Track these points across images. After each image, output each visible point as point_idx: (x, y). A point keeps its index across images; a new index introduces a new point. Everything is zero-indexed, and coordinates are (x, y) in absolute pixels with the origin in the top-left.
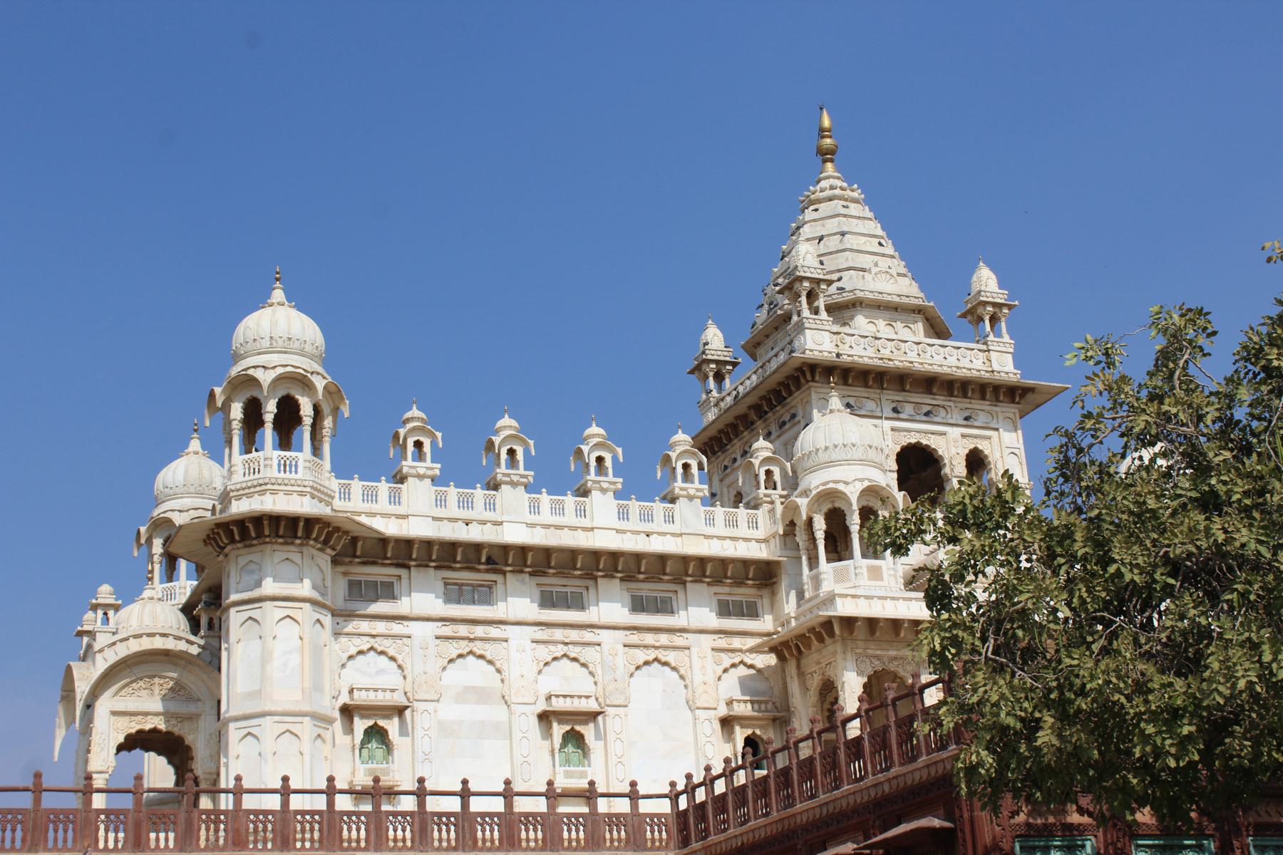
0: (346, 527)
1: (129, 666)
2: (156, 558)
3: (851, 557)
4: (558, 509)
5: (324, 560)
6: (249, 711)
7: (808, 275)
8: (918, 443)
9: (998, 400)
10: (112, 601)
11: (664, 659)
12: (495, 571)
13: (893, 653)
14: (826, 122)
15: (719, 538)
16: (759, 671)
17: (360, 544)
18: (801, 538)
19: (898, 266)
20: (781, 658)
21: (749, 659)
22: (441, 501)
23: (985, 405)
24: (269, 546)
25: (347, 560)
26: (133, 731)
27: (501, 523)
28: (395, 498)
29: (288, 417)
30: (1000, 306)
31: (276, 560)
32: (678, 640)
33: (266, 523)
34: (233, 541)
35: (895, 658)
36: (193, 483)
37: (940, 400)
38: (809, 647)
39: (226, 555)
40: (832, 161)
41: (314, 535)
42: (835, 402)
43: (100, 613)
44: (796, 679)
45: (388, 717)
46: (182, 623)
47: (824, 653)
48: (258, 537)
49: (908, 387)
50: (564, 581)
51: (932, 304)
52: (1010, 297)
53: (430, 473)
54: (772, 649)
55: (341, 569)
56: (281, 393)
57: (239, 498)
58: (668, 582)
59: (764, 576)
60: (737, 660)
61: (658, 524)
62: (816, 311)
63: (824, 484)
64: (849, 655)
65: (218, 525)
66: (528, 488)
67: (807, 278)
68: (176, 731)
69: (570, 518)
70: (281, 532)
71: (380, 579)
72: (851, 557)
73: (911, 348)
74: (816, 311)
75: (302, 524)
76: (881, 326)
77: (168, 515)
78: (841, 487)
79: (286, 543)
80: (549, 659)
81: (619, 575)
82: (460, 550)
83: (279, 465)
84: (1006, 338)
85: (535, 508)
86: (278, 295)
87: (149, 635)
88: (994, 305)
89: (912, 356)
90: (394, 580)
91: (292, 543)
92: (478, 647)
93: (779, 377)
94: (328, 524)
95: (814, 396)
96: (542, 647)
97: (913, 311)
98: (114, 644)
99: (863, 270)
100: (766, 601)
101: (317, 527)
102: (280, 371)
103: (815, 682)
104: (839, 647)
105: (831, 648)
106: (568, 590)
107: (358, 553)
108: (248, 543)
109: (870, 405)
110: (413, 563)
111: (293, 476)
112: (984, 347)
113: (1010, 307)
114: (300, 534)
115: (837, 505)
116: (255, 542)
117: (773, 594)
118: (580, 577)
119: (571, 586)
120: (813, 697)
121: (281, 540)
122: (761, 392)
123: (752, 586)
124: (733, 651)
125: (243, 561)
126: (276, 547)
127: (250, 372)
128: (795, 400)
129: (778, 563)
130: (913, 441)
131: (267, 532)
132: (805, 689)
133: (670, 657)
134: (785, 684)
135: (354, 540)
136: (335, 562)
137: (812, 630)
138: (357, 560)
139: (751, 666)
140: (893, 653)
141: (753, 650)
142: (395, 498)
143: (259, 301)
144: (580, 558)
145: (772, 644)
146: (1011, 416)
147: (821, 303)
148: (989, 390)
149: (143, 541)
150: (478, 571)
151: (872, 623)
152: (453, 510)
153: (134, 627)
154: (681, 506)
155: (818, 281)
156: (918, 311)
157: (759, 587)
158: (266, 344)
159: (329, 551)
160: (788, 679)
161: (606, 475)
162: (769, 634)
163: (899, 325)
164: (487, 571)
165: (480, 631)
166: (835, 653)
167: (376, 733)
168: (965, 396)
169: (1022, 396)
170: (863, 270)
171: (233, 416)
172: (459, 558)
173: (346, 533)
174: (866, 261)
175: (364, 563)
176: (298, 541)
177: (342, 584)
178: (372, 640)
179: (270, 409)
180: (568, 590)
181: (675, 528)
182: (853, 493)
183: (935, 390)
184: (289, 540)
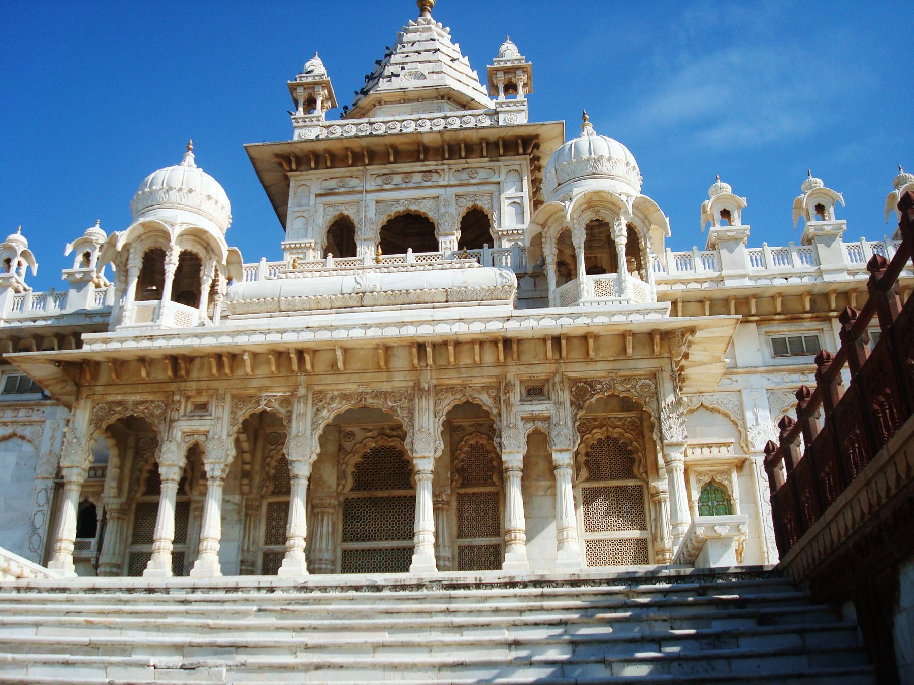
32: (36, 416)
35: (143, 402)
37: (431, 165)
88: (507, 71)
109: (354, 182)
130: (401, 208)
133: (27, 432)
140: (138, 398)
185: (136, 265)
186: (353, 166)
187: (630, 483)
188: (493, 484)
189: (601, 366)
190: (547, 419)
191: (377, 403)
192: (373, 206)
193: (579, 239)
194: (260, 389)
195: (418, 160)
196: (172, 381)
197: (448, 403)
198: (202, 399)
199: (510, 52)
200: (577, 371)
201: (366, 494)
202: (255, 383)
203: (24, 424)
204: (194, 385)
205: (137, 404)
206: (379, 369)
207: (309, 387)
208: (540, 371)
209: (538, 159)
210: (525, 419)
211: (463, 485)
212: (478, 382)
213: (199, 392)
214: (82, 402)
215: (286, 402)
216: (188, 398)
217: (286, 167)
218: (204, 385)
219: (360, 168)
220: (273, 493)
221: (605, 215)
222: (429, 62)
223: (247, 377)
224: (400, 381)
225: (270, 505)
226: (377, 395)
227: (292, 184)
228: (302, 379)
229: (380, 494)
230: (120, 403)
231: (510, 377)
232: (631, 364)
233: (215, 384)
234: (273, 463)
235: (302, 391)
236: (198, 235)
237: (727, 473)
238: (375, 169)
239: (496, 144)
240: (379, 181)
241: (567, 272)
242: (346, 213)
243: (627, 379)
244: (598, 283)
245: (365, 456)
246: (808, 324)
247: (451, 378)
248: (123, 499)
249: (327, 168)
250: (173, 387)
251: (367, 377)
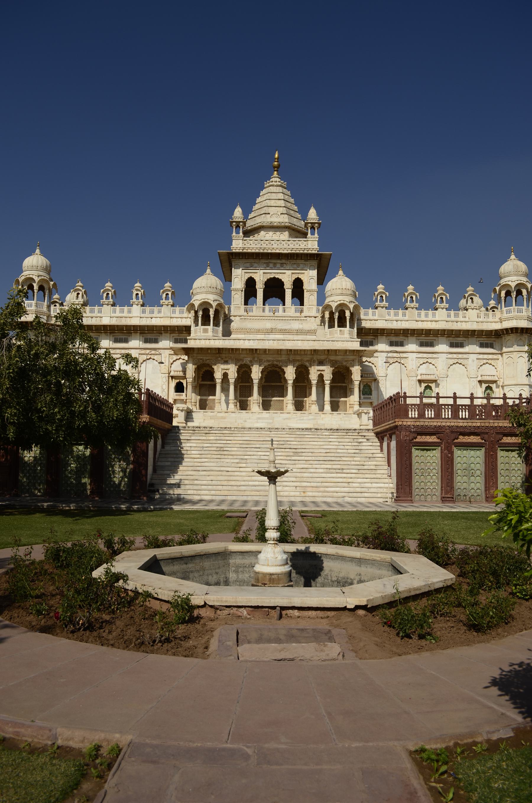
4: (122, 311)
8: (274, 278)
14: (276, 156)
23: (303, 262)
27: (102, 317)
37: (283, 261)
40: (277, 171)
61: (156, 314)
74: (237, 233)
84: (316, 235)
85: (114, 312)
86: (38, 251)
89: (275, 246)
109: (256, 265)
130: (272, 277)
139: (183, 359)
146: (314, 264)
154: (164, 309)
163: (278, 233)
181: (162, 315)
185: (200, 313)
186: (256, 259)
187: (344, 385)
188: (305, 383)
189: (339, 357)
190: (324, 371)
191: (277, 363)
192: (262, 274)
193: (336, 316)
194: (244, 357)
195: (279, 259)
196: (217, 354)
197: (297, 364)
198: (227, 359)
199: (312, 215)
200: (333, 358)
201: (269, 384)
202: (242, 356)
203: (154, 354)
204: (224, 355)
205: (206, 360)
206: (278, 354)
207: (258, 358)
208: (322, 357)
209: (320, 259)
210: (318, 371)
211: (296, 383)
212: (306, 359)
213: (226, 358)
215: (251, 361)
216: (222, 359)
217: (231, 257)
218: (227, 355)
220: (241, 382)
221: (344, 308)
222: (281, 207)
223: (240, 354)
224: (284, 358)
225: (240, 386)
226: (278, 361)
227: (233, 264)
228: (256, 355)
229: (273, 384)
230: (201, 359)
231: (315, 358)
232: (348, 357)
233: (231, 355)
234: (241, 373)
235: (256, 359)
236: (220, 305)
237: (371, 382)
238: (263, 261)
240: (265, 265)
241: (331, 326)
242: (253, 276)
243: (346, 361)
244: (341, 331)
245: (268, 372)
246: (401, 337)
247: (298, 358)
248: (196, 383)
249: (246, 259)
250: (218, 355)
251: (274, 356)
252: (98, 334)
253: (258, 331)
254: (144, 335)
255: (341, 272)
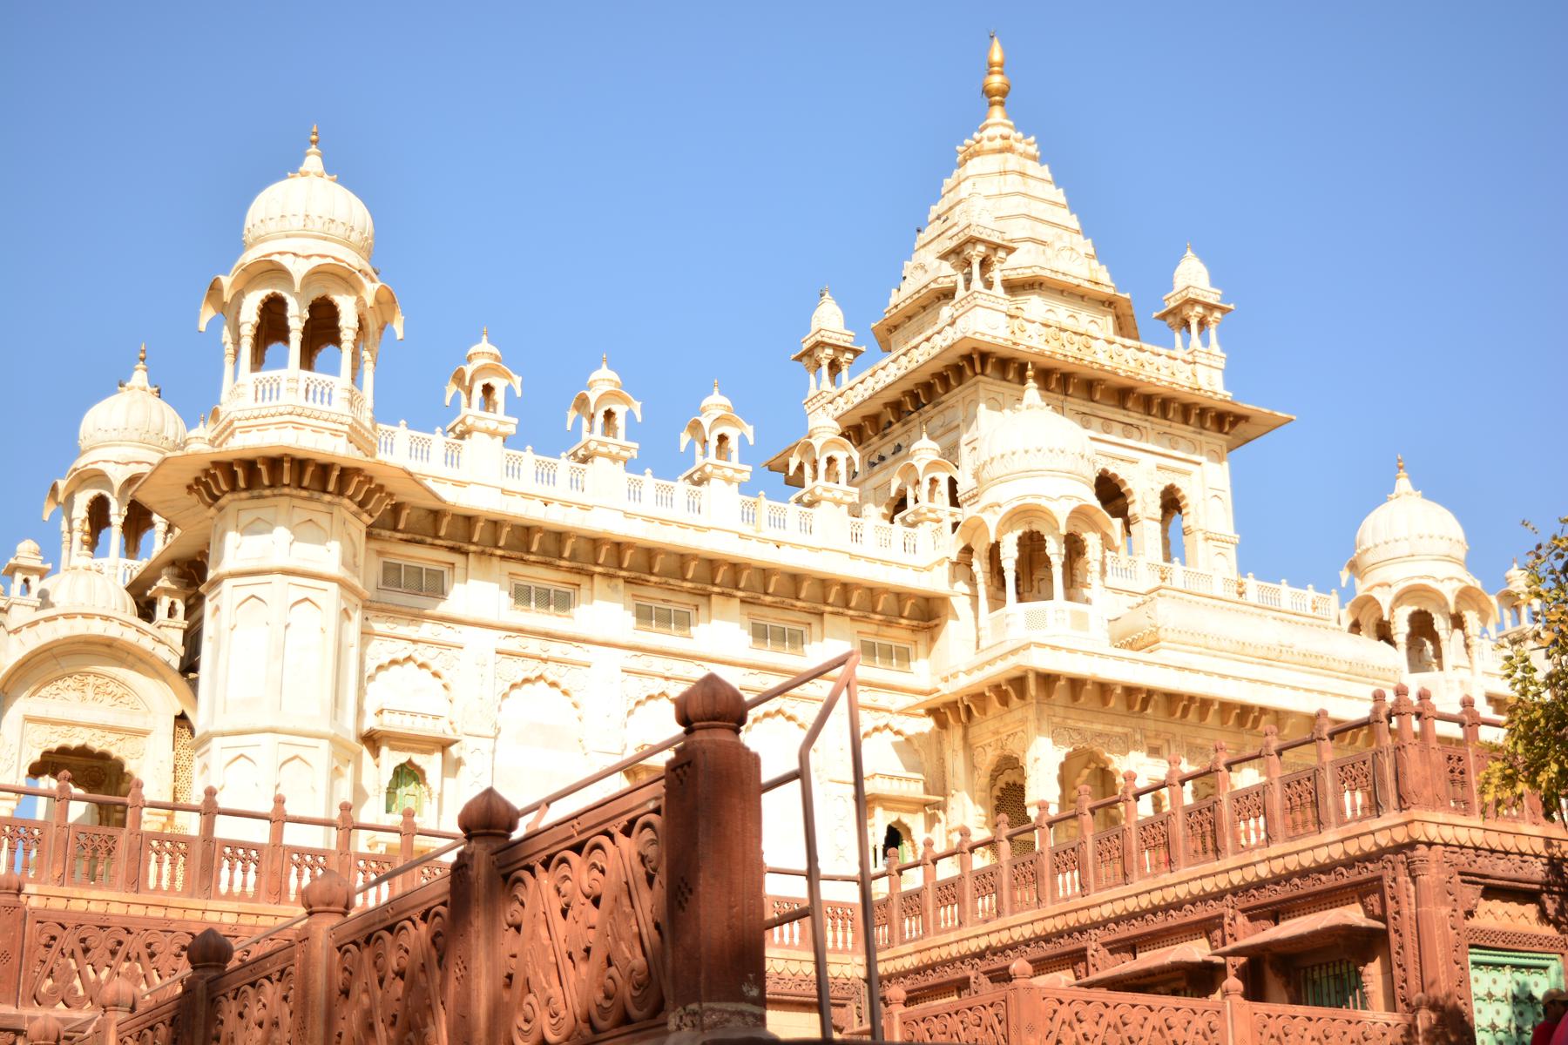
0: (391, 486)
1: (55, 657)
2: (76, 524)
3: (1050, 597)
4: (666, 499)
5: (358, 528)
6: (241, 726)
7: (984, 237)
9: (1203, 427)
10: (36, 563)
11: (789, 712)
12: (579, 571)
13: (1098, 727)
14: (997, 55)
15: (868, 559)
16: (908, 740)
17: (404, 514)
18: (979, 567)
19: (1087, 246)
20: (942, 724)
21: (898, 722)
22: (513, 470)
23: (1188, 431)
24: (284, 501)
25: (386, 533)
26: (54, 747)
28: (452, 459)
29: (323, 327)
30: (1210, 308)
31: (296, 520)
33: (286, 466)
34: (234, 488)
35: (1100, 735)
36: (127, 431)
37: (1135, 417)
38: (984, 711)
39: (221, 509)
40: (1002, 104)
41: (350, 492)
42: (1032, 390)
43: (19, 577)
44: (961, 754)
45: (429, 752)
46: (125, 606)
47: (1008, 718)
48: (272, 486)
49: (1098, 397)
50: (667, 595)
51: (1127, 296)
52: (1224, 298)
53: (503, 429)
54: (932, 712)
55: (375, 545)
56: (315, 294)
57: (247, 430)
58: (802, 610)
59: (927, 614)
60: (881, 723)
62: (989, 285)
63: (1019, 498)
64: (1044, 723)
65: (216, 464)
66: (630, 466)
67: (983, 241)
68: (115, 752)
69: (679, 511)
70: (306, 483)
71: (425, 565)
72: (1050, 597)
73: (1101, 348)
75: (336, 473)
76: (1061, 312)
77: (100, 466)
78: (1043, 503)
79: (310, 499)
80: (643, 697)
81: (740, 594)
82: (537, 537)
83: (307, 391)
84: (1215, 347)
85: (635, 494)
86: (313, 162)
87: (85, 616)
89: (1103, 359)
90: (444, 568)
91: (318, 500)
92: (551, 672)
93: (938, 366)
94: (370, 479)
95: (982, 393)
96: (632, 677)
97: (1103, 303)
98: (36, 623)
99: (1043, 243)
100: (921, 648)
101: (356, 480)
102: (316, 261)
103: (988, 759)
104: (1031, 713)
105: (1018, 714)
106: (673, 607)
107: (401, 526)
108: (256, 493)
110: (472, 548)
111: (325, 407)
112: (1189, 358)
113: (1224, 311)
114: (331, 487)
115: (1035, 528)
116: (267, 492)
117: (933, 639)
118: (690, 592)
119: (679, 603)
120: (983, 779)
121: (304, 493)
122: (908, 385)
123: (906, 628)
124: (877, 709)
125: (246, 517)
126: (297, 502)
127: (276, 258)
128: (958, 394)
129: (944, 600)
131: (286, 480)
132: (972, 767)
134: (942, 760)
135: (397, 509)
136: (369, 536)
137: (997, 688)
138: (399, 535)
139: (898, 733)
140: (1098, 727)
141: (906, 712)
142: (452, 459)
143: (288, 165)
144: (693, 564)
145: (933, 705)
146: (1217, 448)
147: (996, 275)
148: (1195, 412)
149: (61, 498)
150: (558, 568)
151: (1076, 684)
152: (527, 482)
153: (81, 602)
155: (996, 247)
156: (1108, 303)
157: (914, 630)
158: (296, 224)
159: (365, 517)
160: (948, 755)
161: (728, 459)
162: (930, 693)
164: (570, 570)
165: (556, 649)
166: (1024, 721)
167: (407, 774)
168: (1165, 416)
169: (1233, 424)
170: (1043, 243)
171: (242, 318)
172: (534, 548)
173: (390, 495)
174: (1044, 232)
175: (413, 541)
176: (327, 498)
177: (376, 567)
178: (411, 647)
179: (296, 317)
180: (673, 607)
182: (1062, 513)
183: (1129, 405)
184: (316, 495)
198: (1158, 743)
213: (1157, 736)
214: (1044, 723)
219: (1062, 397)
228: (1247, 737)
230: (1078, 731)
239: (1203, 412)
252: (576, 578)
253: (1241, 651)
254: (756, 610)
255: (1403, 484)
